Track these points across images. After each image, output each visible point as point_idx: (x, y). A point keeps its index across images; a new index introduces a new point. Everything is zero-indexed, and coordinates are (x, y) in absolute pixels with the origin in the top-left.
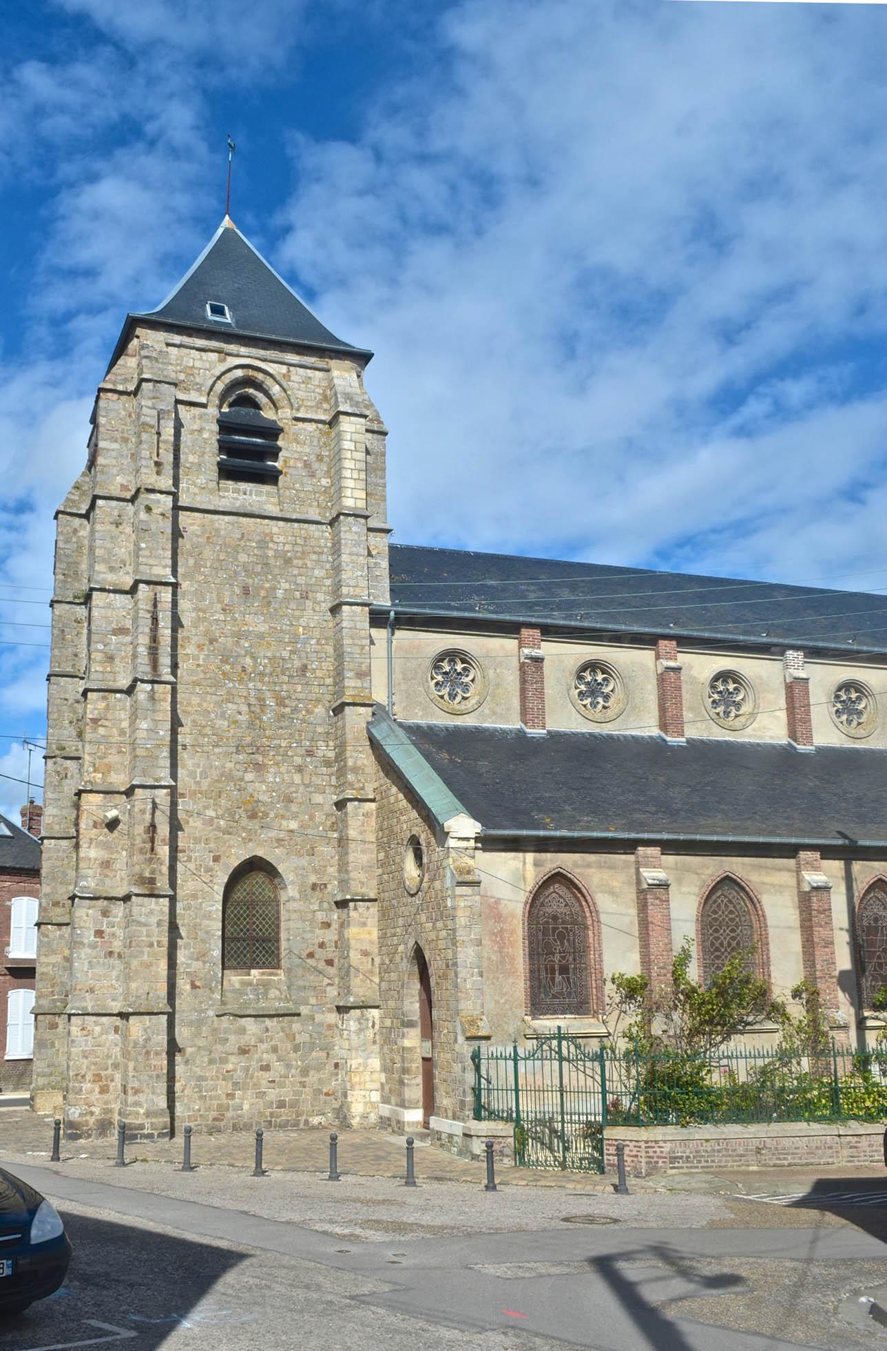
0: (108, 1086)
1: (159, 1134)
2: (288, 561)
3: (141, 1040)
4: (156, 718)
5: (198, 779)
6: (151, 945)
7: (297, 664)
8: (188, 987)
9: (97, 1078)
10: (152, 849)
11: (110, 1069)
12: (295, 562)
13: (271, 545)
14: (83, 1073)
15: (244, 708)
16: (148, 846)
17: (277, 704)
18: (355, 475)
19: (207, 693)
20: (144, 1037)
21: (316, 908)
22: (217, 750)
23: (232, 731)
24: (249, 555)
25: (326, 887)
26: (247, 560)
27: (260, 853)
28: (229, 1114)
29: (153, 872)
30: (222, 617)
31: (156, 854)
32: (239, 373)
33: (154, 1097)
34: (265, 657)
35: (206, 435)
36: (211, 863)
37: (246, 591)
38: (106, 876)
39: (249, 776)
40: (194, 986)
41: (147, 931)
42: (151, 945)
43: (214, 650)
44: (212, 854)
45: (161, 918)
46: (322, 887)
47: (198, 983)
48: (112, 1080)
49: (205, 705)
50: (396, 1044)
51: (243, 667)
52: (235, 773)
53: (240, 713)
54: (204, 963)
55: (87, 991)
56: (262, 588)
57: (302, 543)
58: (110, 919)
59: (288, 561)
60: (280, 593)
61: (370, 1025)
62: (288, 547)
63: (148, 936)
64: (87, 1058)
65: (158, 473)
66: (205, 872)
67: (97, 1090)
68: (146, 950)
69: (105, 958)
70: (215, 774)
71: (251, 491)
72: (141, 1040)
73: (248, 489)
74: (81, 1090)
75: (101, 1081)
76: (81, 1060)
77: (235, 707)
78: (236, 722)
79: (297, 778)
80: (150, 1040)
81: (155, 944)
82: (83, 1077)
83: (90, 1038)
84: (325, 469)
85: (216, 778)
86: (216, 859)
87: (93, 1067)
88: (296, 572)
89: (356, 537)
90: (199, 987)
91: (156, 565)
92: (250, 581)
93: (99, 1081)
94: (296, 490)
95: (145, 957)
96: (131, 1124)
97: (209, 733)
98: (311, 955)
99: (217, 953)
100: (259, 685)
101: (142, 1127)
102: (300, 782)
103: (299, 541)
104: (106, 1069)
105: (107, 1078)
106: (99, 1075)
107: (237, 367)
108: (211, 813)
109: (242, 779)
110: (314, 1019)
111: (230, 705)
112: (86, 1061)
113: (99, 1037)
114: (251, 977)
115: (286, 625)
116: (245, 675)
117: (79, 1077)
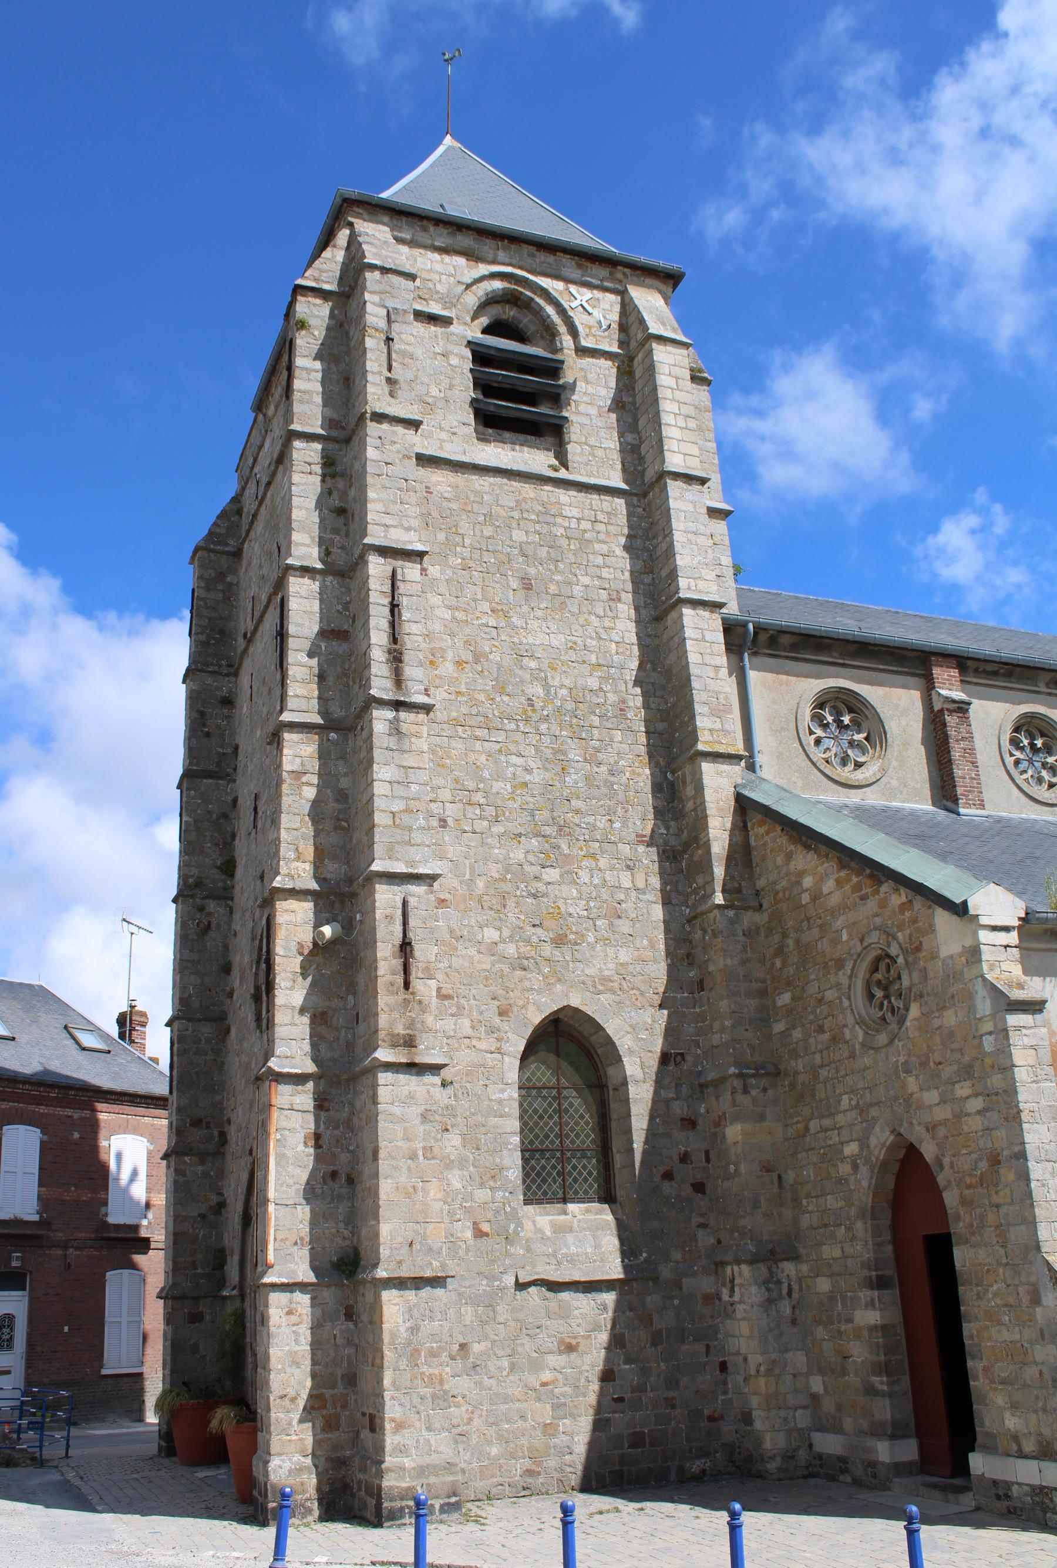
0: (337, 1417)
1: (442, 1506)
2: (585, 543)
3: (402, 1329)
4: (405, 764)
5: (467, 876)
6: (413, 1157)
7: (612, 698)
8: (469, 1234)
10: (407, 985)
11: (340, 1385)
12: (597, 546)
13: (559, 520)
16: (400, 980)
17: (586, 760)
18: (681, 422)
19: (477, 739)
20: (408, 1324)
21: (671, 1095)
23: (519, 799)
25: (684, 1060)
26: (524, 539)
27: (575, 1001)
28: (552, 1463)
29: (411, 1025)
30: (492, 622)
31: (413, 993)
32: (498, 285)
33: (432, 1438)
34: (562, 686)
35: (454, 361)
37: (527, 585)
39: (552, 874)
40: (479, 1234)
41: (405, 1129)
42: (413, 1157)
43: (482, 671)
44: (497, 1003)
45: (428, 1107)
46: (679, 1058)
47: (485, 1227)
48: (345, 1406)
49: (472, 757)
50: (850, 1321)
51: (529, 699)
52: (528, 868)
55: (296, 1243)
56: (552, 580)
57: (606, 521)
58: (331, 1113)
59: (585, 543)
60: (577, 590)
61: (785, 1291)
62: (585, 525)
63: (407, 1139)
65: (392, 395)
66: (487, 1033)
68: (404, 1164)
69: (325, 1182)
70: (495, 871)
72: (402, 1329)
75: (325, 1407)
76: (288, 1370)
77: (519, 761)
79: (626, 880)
80: (418, 1329)
81: (420, 1153)
84: (630, 420)
85: (497, 876)
88: (600, 560)
89: (691, 508)
90: (487, 1235)
91: (395, 527)
92: (532, 571)
93: (319, 1408)
94: (591, 447)
95: (403, 1179)
97: (482, 801)
98: (668, 1176)
100: (555, 729)
102: (631, 885)
103: (600, 517)
105: (334, 1402)
107: (494, 276)
108: (491, 934)
110: (680, 1288)
114: (569, 1217)
115: (591, 638)
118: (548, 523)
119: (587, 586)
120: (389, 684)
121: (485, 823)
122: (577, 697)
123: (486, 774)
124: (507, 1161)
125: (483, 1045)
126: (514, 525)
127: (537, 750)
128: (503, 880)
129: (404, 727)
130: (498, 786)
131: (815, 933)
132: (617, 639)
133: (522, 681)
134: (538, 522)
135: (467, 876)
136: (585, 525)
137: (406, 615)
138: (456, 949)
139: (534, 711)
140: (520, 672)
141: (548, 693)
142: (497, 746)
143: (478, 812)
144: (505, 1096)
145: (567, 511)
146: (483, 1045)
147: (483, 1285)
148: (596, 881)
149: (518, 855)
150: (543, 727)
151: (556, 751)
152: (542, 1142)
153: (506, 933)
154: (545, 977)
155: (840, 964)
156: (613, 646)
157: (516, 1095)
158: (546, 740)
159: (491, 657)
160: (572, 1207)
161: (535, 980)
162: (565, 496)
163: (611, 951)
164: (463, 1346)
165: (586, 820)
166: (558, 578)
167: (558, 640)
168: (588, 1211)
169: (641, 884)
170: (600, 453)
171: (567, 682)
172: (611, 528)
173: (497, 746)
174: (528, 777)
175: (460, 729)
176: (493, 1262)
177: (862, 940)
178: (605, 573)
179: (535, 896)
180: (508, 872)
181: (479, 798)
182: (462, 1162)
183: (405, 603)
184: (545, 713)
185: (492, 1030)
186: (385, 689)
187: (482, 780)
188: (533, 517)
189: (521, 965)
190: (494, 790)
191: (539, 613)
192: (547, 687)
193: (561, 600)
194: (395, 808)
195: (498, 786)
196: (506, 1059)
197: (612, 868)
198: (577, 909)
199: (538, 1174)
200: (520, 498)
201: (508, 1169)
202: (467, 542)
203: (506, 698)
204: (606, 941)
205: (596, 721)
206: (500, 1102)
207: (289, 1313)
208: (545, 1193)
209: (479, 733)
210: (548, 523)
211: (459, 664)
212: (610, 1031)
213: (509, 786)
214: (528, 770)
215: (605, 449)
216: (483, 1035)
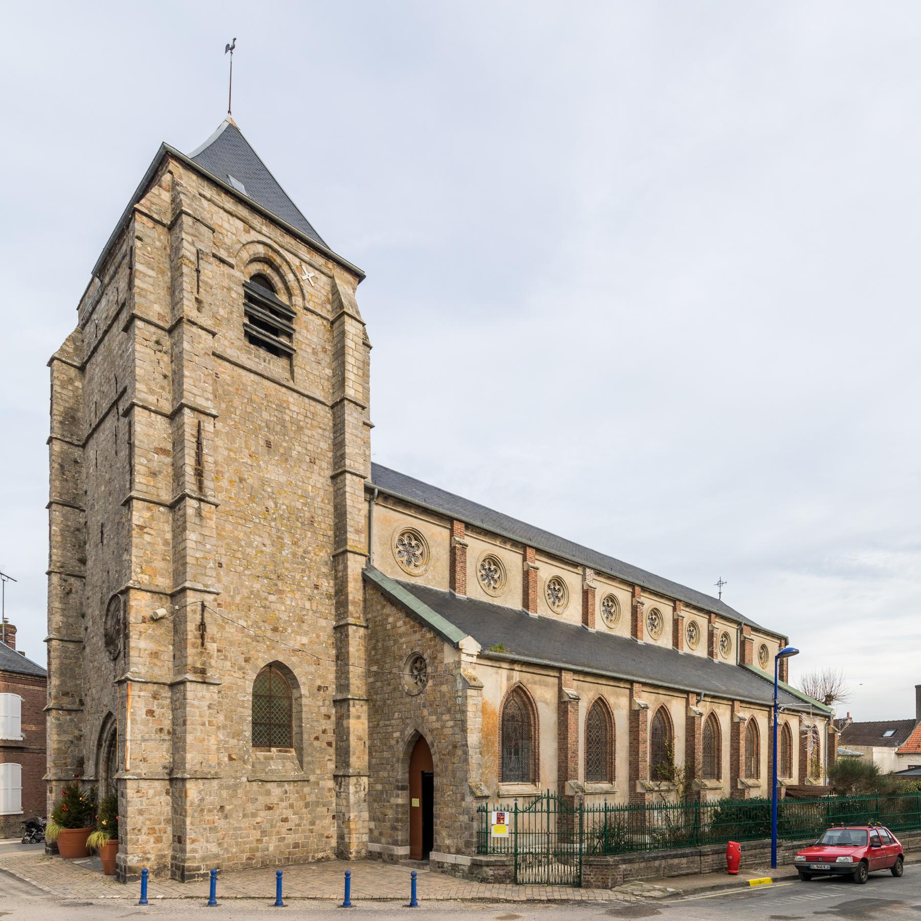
0: (161, 837)
5: (232, 594)
8: (226, 759)
9: (152, 831)
13: (287, 411)
14: (139, 828)
15: (268, 542)
19: (239, 524)
22: (247, 572)
23: (259, 558)
24: (270, 414)
26: (268, 418)
36: (243, 664)
37: (268, 444)
38: (155, 665)
40: (231, 759)
44: (243, 656)
47: (234, 756)
48: (165, 832)
49: (236, 533)
52: (261, 593)
53: (264, 545)
54: (238, 740)
64: (142, 815)
67: (152, 840)
69: (156, 733)
70: (245, 592)
71: (269, 361)
73: (267, 358)
74: (138, 840)
76: (137, 817)
78: (262, 552)
82: (139, 830)
83: (144, 799)
86: (247, 660)
87: (148, 822)
96: (189, 866)
97: (240, 556)
99: (248, 734)
101: (198, 868)
104: (160, 824)
106: (153, 829)
108: (242, 623)
109: (266, 599)
111: (257, 538)
112: (141, 818)
113: (153, 797)
116: (269, 514)
117: (136, 831)
118: (281, 412)
119: (299, 452)
120: (195, 488)
121: (242, 568)
122: (291, 510)
123: (243, 543)
124: (245, 728)
125: (236, 675)
126: (264, 408)
127: (269, 535)
128: (249, 598)
129: (203, 514)
130: (248, 550)
131: (392, 643)
132: (312, 484)
133: (264, 497)
134: (277, 410)
135: (232, 594)
136: (301, 417)
137: (205, 451)
138: (225, 628)
139: (269, 514)
140: (263, 493)
141: (276, 506)
142: (249, 530)
143: (238, 562)
144: (246, 699)
145: (292, 408)
146: (236, 675)
147: (232, 781)
148: (294, 604)
149: (257, 586)
150: (273, 524)
151: (279, 537)
152: (261, 720)
153: (250, 623)
154: (268, 646)
155: (401, 658)
156: (310, 487)
157: (251, 699)
158: (274, 531)
159: (248, 481)
160: (273, 749)
161: (262, 647)
162: (292, 398)
163: (298, 638)
164: (222, 807)
165: (291, 574)
166: (285, 444)
167: (283, 479)
168: (280, 751)
169: (314, 608)
170: (311, 377)
171: (286, 502)
172: (313, 422)
173: (249, 530)
174: (264, 548)
175: (230, 517)
176: (237, 771)
177: (412, 650)
178: (309, 447)
179: (264, 607)
180: (252, 594)
181: (239, 555)
182: (225, 727)
183: (205, 443)
184: (274, 516)
185: (240, 668)
186: (193, 491)
187: (242, 546)
188: (274, 406)
189: (256, 638)
190: (247, 552)
191: (274, 462)
192: (276, 504)
193: (285, 457)
194: (198, 555)
195: (248, 550)
196: (247, 682)
197: (302, 599)
198: (284, 617)
199: (258, 734)
200: (268, 393)
201: (246, 731)
202: (238, 413)
203: (255, 505)
204: (298, 634)
205: (299, 525)
206: (243, 701)
207: (138, 792)
208: (261, 742)
209: (240, 521)
210: (281, 412)
211: (231, 482)
212: (295, 674)
213: (254, 551)
214: (264, 545)
215: (314, 375)
216: (236, 670)
